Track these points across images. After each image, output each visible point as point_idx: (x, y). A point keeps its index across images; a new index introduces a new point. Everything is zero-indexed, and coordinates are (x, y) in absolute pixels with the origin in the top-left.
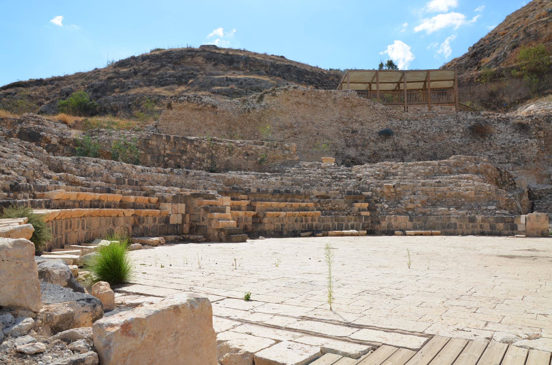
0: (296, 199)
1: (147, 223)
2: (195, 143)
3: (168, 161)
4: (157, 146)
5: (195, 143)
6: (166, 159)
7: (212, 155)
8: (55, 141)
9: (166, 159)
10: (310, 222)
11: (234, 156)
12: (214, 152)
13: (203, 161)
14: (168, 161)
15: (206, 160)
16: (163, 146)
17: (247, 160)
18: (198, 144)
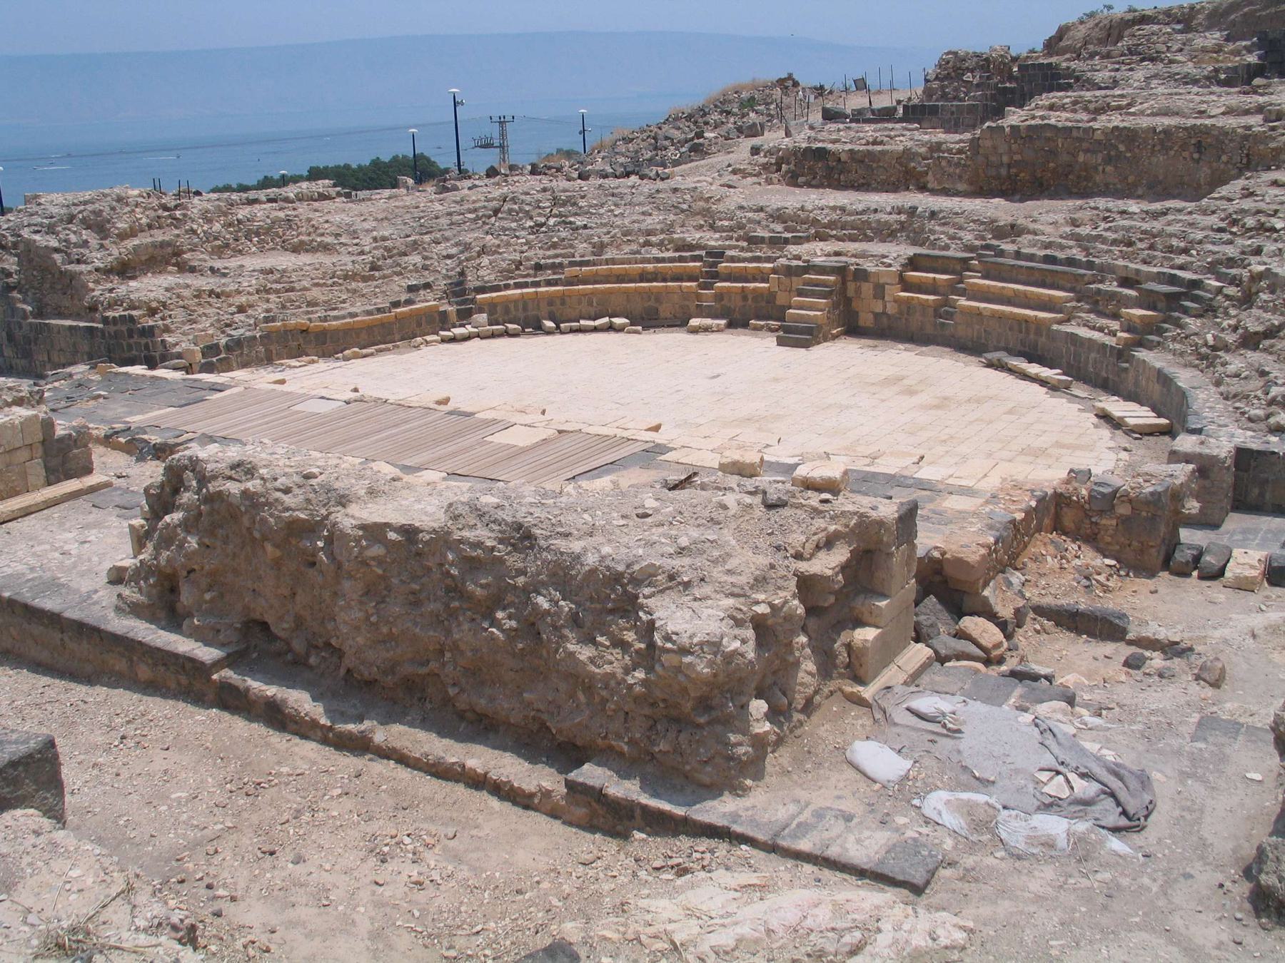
0: (1061, 282)
1: (730, 300)
2: (1075, 134)
3: (1017, 175)
4: (995, 148)
5: (1075, 134)
6: (1013, 171)
7: (1119, 155)
8: (844, 157)
9: (1013, 171)
10: (1032, 336)
11: (1172, 153)
12: (1122, 148)
13: (1096, 168)
14: (1017, 175)
15: (1100, 168)
16: (1006, 147)
17: (1197, 161)
18: (1081, 134)
